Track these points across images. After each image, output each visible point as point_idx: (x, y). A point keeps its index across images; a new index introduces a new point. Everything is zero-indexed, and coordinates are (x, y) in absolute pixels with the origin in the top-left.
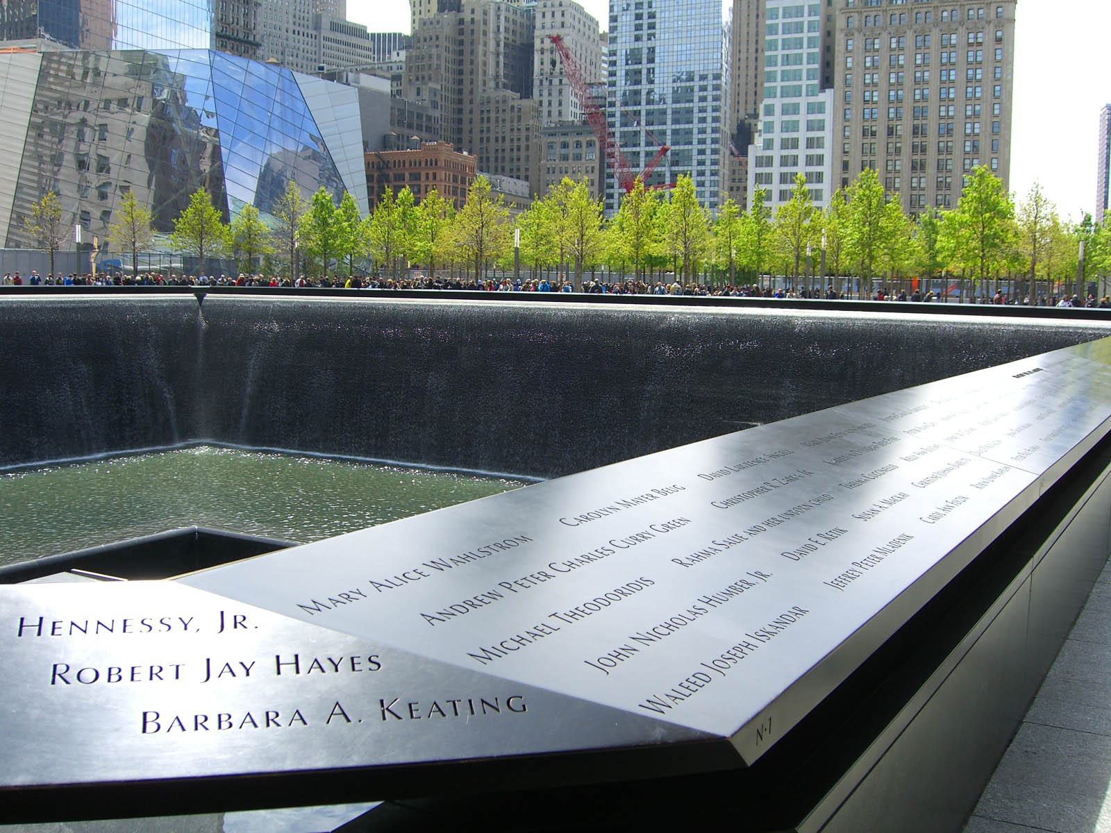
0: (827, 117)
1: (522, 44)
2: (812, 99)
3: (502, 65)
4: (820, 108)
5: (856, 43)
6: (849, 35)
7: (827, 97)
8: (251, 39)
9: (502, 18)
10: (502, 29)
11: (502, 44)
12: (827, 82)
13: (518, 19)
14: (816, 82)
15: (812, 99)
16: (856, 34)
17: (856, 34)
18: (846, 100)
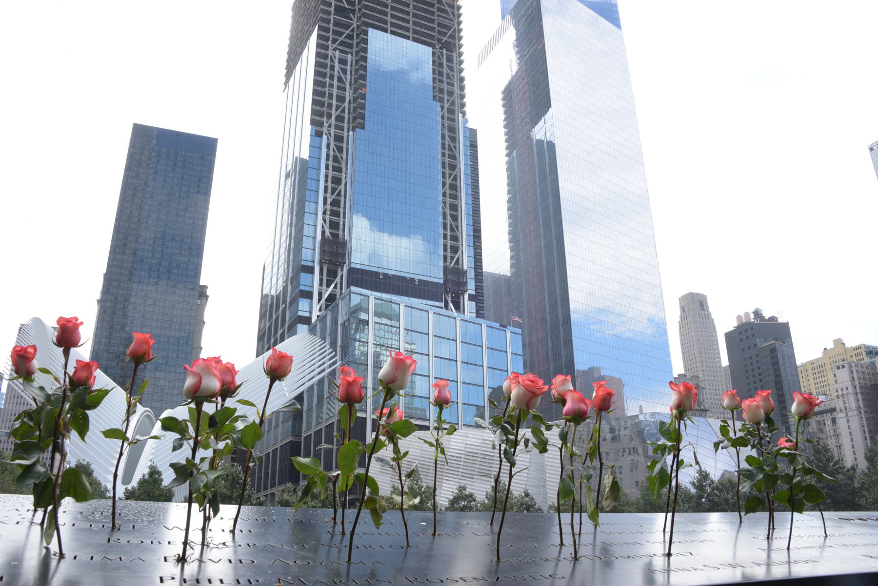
1: (872, 385)
3: (860, 399)
8: (702, 407)
9: (854, 371)
10: (856, 378)
11: (858, 387)
13: (866, 371)
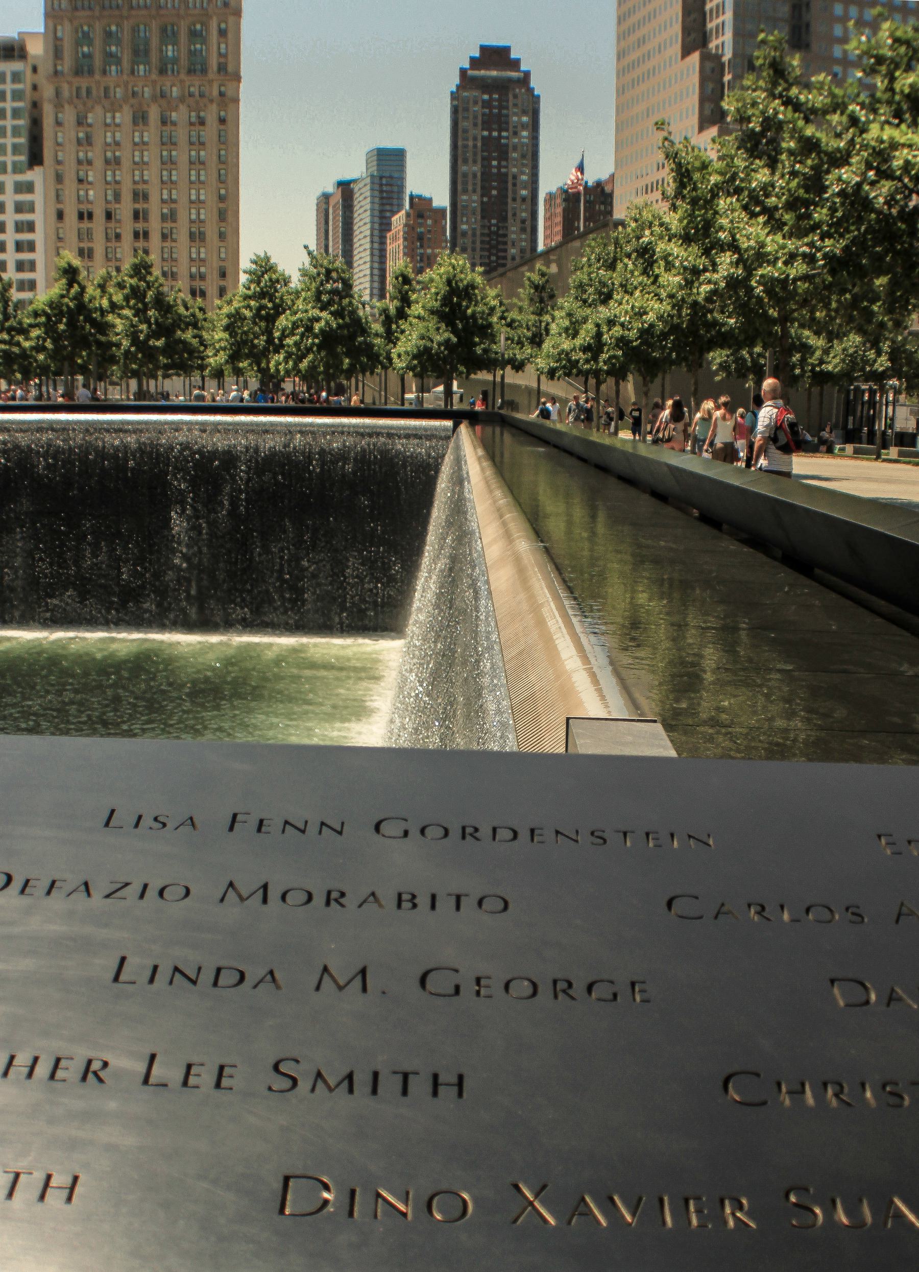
0: (37, 198)
2: (20, 178)
4: (28, 187)
5: (69, 116)
6: (59, 106)
7: (35, 176)
12: (35, 158)
14: (23, 158)
15: (20, 178)
16: (66, 106)
17: (66, 106)
18: (59, 178)
